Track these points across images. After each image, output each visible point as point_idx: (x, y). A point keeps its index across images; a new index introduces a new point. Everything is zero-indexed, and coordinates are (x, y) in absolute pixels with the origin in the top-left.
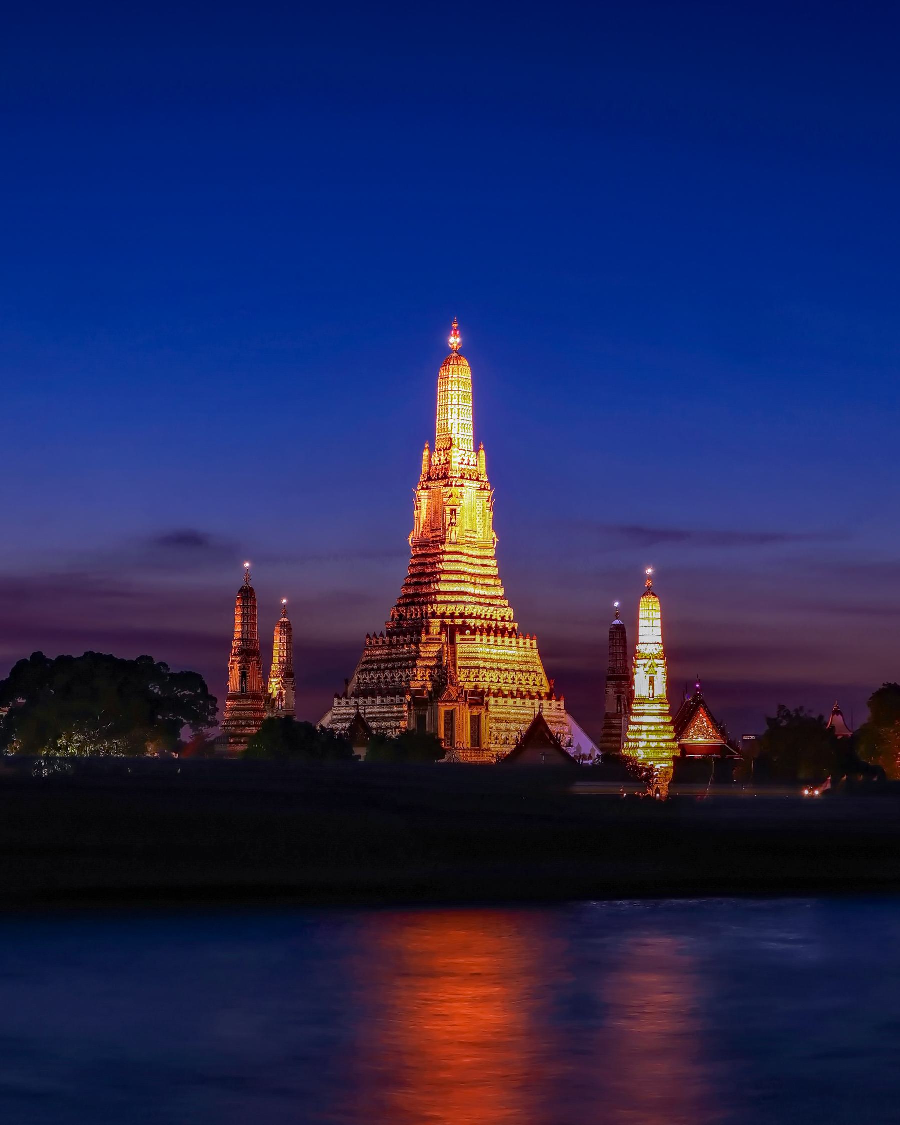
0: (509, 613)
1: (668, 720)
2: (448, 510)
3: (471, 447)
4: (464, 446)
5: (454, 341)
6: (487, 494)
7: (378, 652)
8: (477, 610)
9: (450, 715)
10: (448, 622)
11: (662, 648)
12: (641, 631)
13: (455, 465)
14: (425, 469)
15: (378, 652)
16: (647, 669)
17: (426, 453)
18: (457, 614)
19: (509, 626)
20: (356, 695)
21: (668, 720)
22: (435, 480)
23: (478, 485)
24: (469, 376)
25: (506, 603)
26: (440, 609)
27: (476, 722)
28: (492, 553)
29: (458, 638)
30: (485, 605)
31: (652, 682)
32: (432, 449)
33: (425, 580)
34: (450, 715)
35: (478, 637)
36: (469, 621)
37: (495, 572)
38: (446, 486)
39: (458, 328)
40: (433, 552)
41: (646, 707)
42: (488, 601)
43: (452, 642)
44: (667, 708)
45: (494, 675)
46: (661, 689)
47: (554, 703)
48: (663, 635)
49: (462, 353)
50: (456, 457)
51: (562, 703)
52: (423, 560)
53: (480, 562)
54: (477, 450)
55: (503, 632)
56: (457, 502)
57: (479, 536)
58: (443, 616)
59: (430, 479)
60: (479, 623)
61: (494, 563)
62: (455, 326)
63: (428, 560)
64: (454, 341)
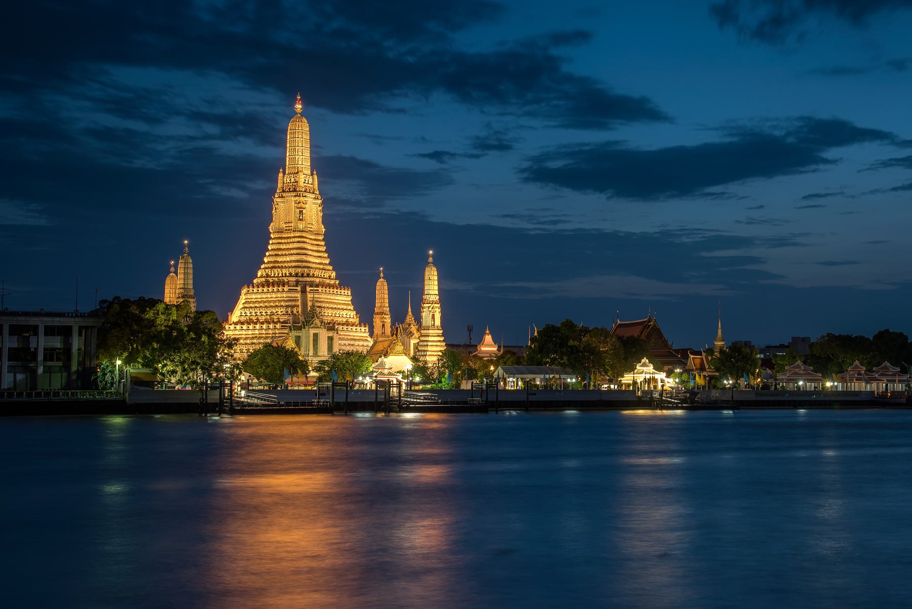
0: (334, 274)
1: (442, 339)
2: (298, 211)
3: (309, 173)
4: (305, 172)
6: (319, 202)
7: (254, 297)
8: (317, 273)
9: (316, 336)
10: (301, 279)
12: (426, 287)
13: (301, 184)
14: (280, 185)
15: (254, 297)
17: (281, 175)
19: (332, 282)
20: (236, 324)
21: (442, 339)
23: (313, 196)
25: (331, 268)
27: (331, 339)
28: (321, 238)
29: (308, 289)
30: (320, 269)
31: (433, 316)
32: (284, 173)
34: (316, 336)
35: (320, 289)
36: (312, 279)
37: (324, 249)
41: (430, 331)
42: (321, 267)
43: (304, 291)
44: (441, 332)
45: (330, 311)
46: (438, 322)
47: (363, 329)
48: (439, 290)
49: (302, 114)
50: (302, 178)
51: (367, 329)
52: (280, 241)
53: (316, 243)
54: (312, 174)
55: (329, 286)
56: (304, 206)
57: (314, 227)
59: (284, 191)
60: (317, 280)
61: (323, 243)
64: (299, 107)
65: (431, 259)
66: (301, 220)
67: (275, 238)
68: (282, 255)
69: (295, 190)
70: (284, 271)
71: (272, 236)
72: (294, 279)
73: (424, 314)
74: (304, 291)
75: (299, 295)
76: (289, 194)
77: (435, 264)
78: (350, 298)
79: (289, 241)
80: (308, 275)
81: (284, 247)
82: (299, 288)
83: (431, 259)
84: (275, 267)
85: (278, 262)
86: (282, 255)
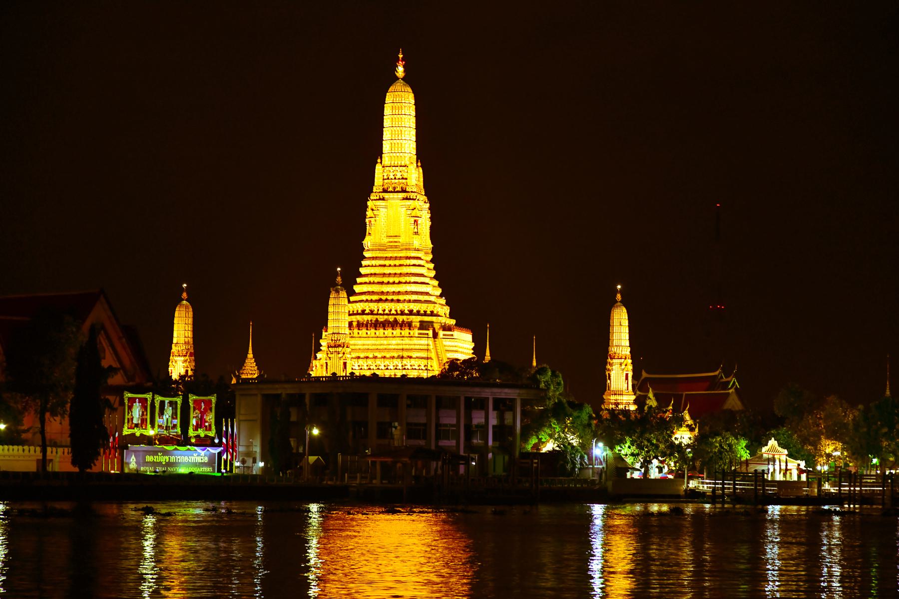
0: (447, 310)
5: (400, 71)
6: (428, 205)
11: (629, 349)
14: (378, 181)
16: (623, 366)
17: (378, 167)
18: (429, 312)
22: (391, 192)
24: (413, 102)
26: (415, 307)
28: (430, 257)
29: (441, 333)
33: (385, 280)
38: (407, 199)
39: (403, 60)
40: (395, 255)
58: (418, 313)
59: (385, 191)
62: (401, 56)
63: (387, 263)
64: (400, 71)
65: (619, 297)
66: (416, 233)
67: (370, 258)
68: (388, 283)
69: (403, 191)
70: (400, 307)
71: (366, 254)
72: (419, 318)
73: (613, 374)
74: (435, 335)
75: (431, 341)
76: (395, 195)
77: (625, 303)
78: (473, 345)
79: (397, 262)
80: (432, 314)
81: (387, 271)
82: (430, 333)
83: (619, 297)
84: (380, 300)
85: (382, 293)
86: (388, 283)
